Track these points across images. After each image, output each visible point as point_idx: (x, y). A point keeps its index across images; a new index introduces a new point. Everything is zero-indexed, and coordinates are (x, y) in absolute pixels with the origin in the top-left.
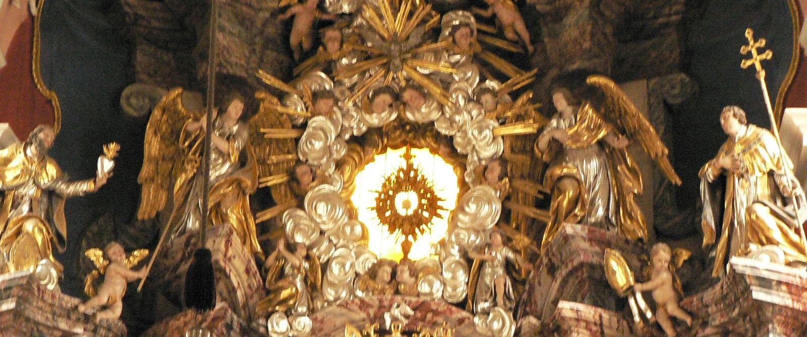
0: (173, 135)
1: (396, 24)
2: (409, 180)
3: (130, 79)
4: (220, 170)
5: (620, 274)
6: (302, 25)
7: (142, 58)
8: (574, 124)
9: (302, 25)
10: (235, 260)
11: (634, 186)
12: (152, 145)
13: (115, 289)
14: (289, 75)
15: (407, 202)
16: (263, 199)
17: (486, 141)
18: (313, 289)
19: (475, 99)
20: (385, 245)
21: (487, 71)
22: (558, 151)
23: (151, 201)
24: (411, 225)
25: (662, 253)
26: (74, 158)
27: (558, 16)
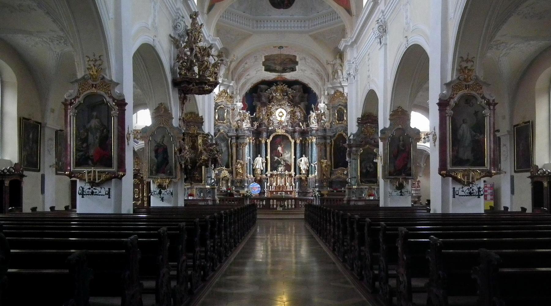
0: (259, 109)
1: (280, 98)
2: (281, 112)
3: (253, 101)
4: (264, 113)
5: (301, 125)
6: (271, 97)
7: (255, 99)
8: (297, 110)
9: (271, 97)
10: (266, 122)
11: (302, 115)
12: (257, 110)
13: (256, 126)
14: (270, 102)
15: (281, 114)
16: (268, 115)
17: (289, 110)
18: (273, 124)
19: (288, 105)
20: (279, 119)
21: (289, 103)
22: (295, 112)
23: (257, 116)
24: (281, 116)
25: (305, 123)
26: (252, 114)
27: (295, 96)
